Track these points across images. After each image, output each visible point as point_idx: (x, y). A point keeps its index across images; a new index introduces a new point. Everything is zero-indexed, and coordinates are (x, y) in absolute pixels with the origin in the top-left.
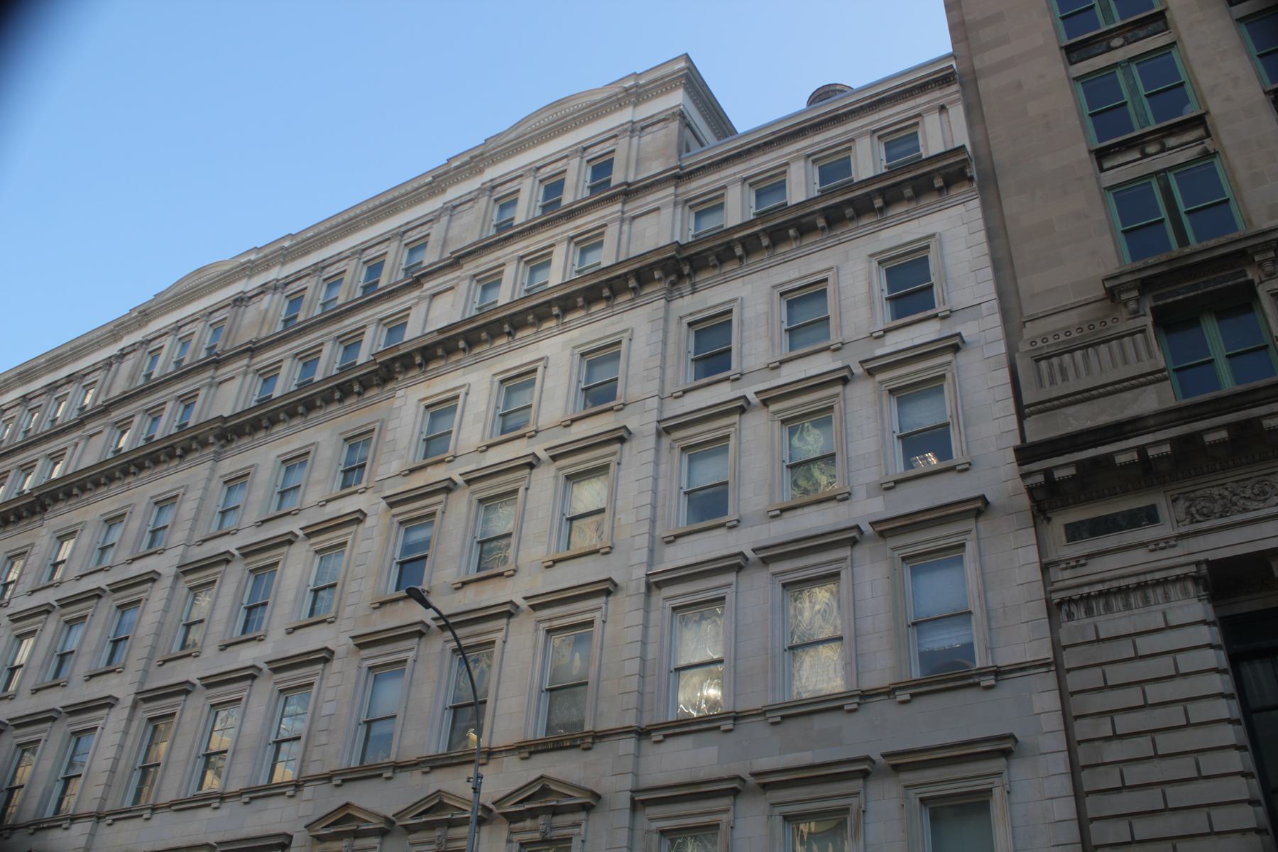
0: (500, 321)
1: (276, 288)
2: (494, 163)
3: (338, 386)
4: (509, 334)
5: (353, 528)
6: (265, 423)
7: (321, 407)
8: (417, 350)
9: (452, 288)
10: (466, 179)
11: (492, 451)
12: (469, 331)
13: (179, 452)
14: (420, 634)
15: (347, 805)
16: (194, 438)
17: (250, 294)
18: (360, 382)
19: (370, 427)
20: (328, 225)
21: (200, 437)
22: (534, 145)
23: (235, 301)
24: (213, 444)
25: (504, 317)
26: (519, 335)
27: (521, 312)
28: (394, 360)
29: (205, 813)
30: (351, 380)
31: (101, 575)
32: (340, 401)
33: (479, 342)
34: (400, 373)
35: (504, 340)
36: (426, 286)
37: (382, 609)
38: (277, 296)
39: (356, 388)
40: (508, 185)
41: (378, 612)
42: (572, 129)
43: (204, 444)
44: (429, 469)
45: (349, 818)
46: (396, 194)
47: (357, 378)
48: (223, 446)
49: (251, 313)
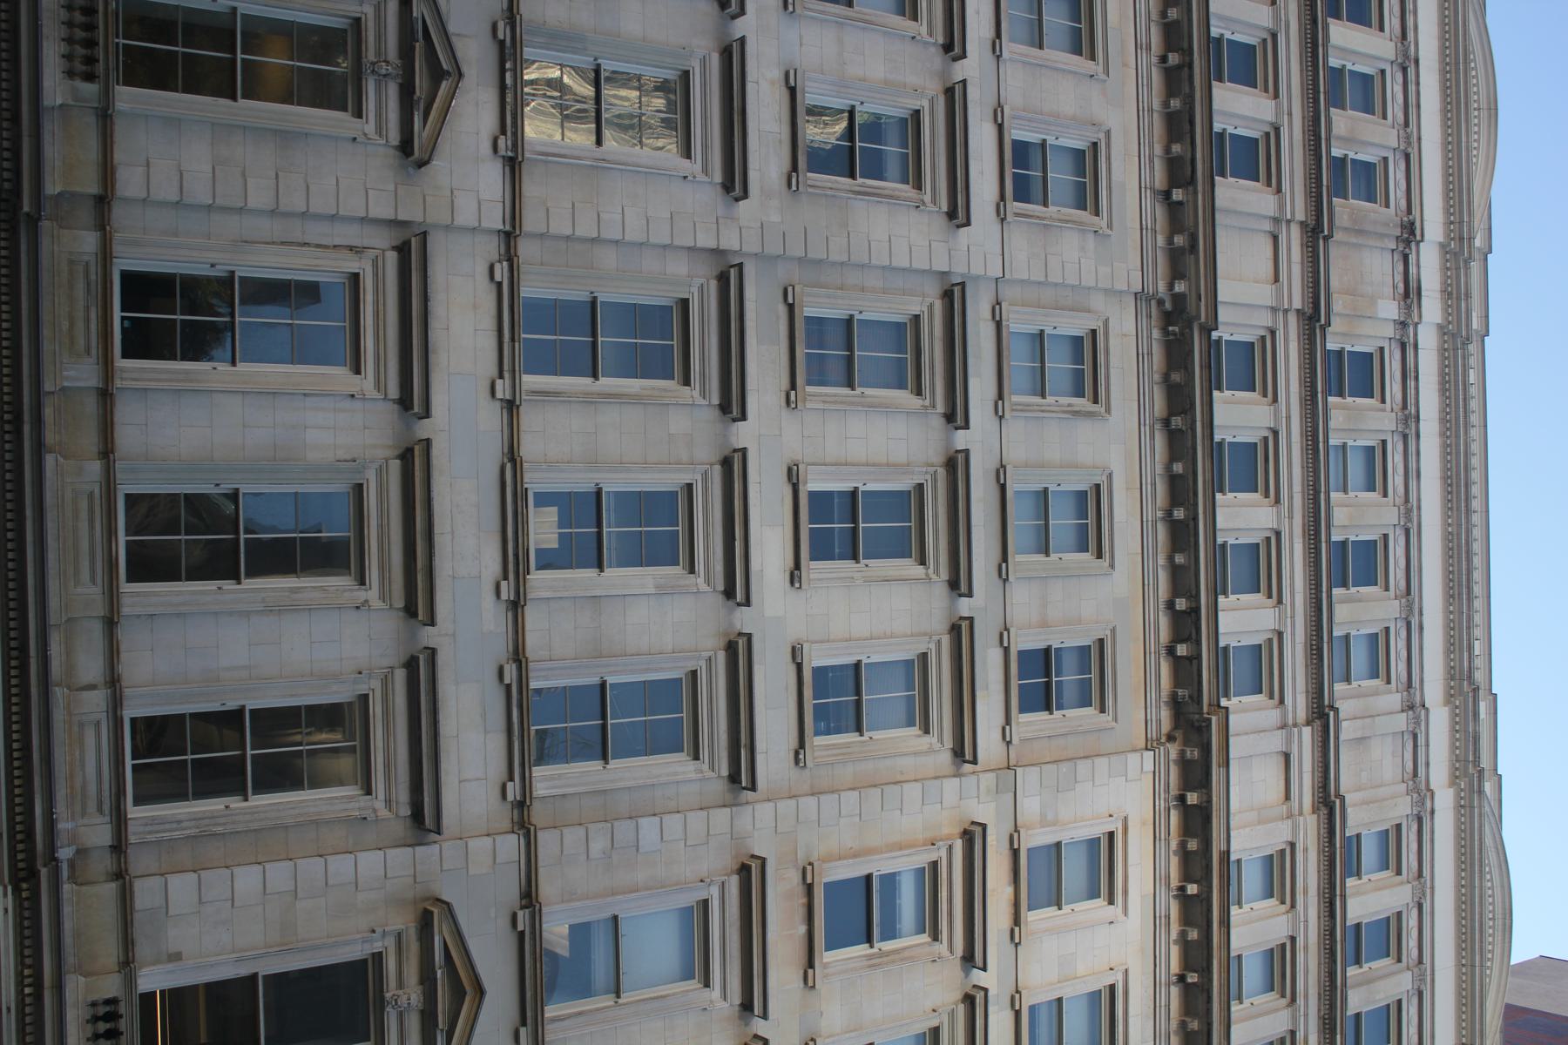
0: (1206, 971)
1: (1403, 325)
2: (1459, 807)
3: (1197, 610)
4: (1181, 978)
5: (949, 743)
6: (1177, 422)
7: (1170, 559)
8: (1209, 801)
9: (1287, 797)
10: (1453, 748)
11: (1009, 1016)
12: (1209, 910)
13: (1178, 195)
14: (747, 1006)
15: (480, 992)
16: (1193, 247)
17: (1412, 259)
18: (1189, 659)
19: (1109, 702)
20: (1475, 447)
21: (1190, 259)
22: (1459, 886)
23: (1412, 224)
24: (1171, 286)
25: (1210, 980)
26: (1175, 991)
27: (1209, 1012)
28: (1206, 749)
29: (491, 563)
30: (1198, 643)
31: (988, 32)
32: (1170, 605)
33: (1186, 920)
34: (1182, 753)
35: (1175, 967)
36: (1307, 731)
37: (800, 890)
38: (1389, 331)
39: (1182, 650)
40: (1414, 846)
41: (795, 877)
42: (1459, 956)
43: (1176, 273)
44: (1010, 890)
45: (458, 993)
46: (1477, 604)
47: (1199, 657)
48: (1160, 302)
49: (1379, 267)
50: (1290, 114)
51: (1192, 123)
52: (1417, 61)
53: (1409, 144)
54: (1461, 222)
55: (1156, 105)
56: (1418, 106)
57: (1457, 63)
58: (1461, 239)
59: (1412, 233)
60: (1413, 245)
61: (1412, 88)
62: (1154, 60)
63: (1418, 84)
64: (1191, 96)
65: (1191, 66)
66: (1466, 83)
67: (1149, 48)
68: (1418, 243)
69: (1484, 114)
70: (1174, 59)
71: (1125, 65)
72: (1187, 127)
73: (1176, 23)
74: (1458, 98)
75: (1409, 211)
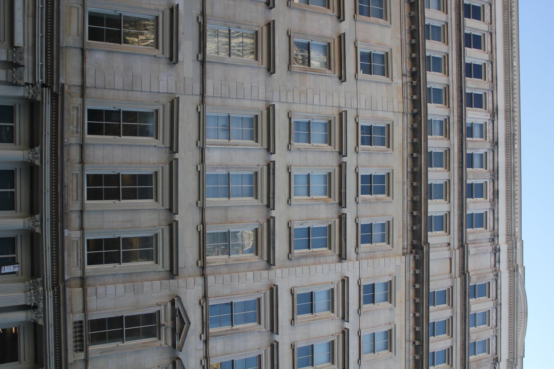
23: (497, 358)
31: (357, 358)
50: (456, 341)
51: (422, 364)
52: (501, 304)
53: (497, 332)
54: (514, 353)
55: (411, 357)
56: (501, 319)
57: (514, 302)
58: (514, 358)
59: (497, 361)
60: (497, 364)
61: (499, 313)
62: (411, 343)
63: (501, 311)
64: (423, 355)
65: (423, 346)
66: (517, 302)
67: (410, 341)
68: (499, 363)
69: (523, 314)
70: (417, 343)
71: (401, 348)
72: (421, 365)
73: (419, 332)
74: (514, 313)
75: (496, 354)
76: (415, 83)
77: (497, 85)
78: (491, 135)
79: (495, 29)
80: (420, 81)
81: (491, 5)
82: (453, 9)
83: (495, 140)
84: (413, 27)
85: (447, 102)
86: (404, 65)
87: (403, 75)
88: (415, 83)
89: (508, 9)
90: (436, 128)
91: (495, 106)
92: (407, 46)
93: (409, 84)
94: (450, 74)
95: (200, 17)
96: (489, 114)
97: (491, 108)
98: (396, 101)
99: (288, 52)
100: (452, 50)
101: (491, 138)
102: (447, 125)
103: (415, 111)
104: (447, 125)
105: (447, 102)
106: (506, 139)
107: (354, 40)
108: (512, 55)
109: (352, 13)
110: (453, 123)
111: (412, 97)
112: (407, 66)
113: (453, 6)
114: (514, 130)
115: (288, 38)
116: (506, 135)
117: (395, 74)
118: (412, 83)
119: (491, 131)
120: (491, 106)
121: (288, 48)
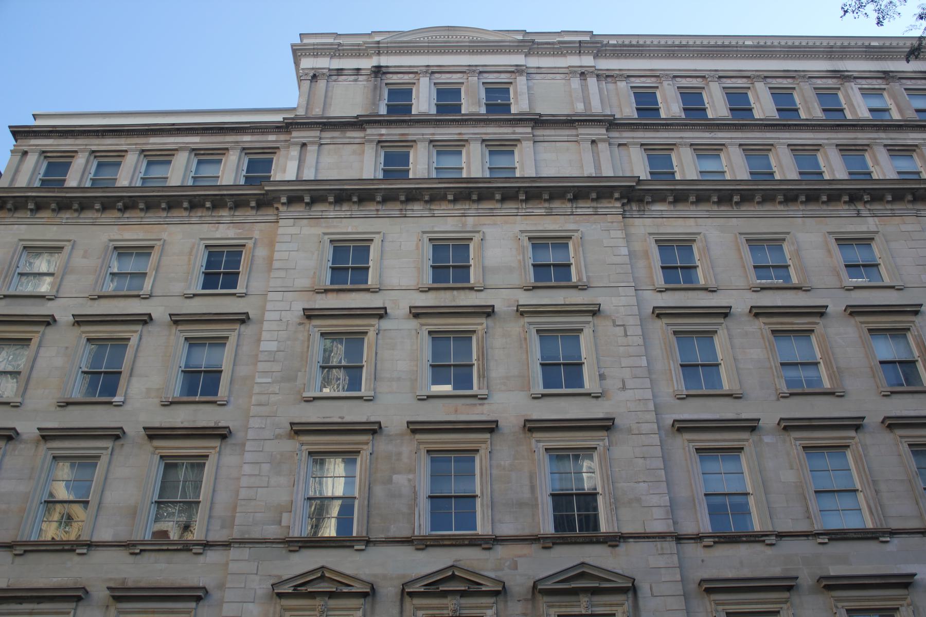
76: (866, 198)
77: (796, 71)
78: (874, 81)
79: (710, 71)
80: (864, 190)
81: (675, 77)
82: (712, 135)
83: (881, 75)
84: (780, 198)
85: (861, 148)
86: (843, 213)
87: (859, 215)
88: (866, 198)
89: (674, 51)
90: (710, 165)
91: (829, 74)
92: (809, 207)
93: (868, 206)
94: (771, 142)
95: (820, 541)
96: (847, 84)
97: (835, 80)
98: (904, 228)
99: (916, 396)
100: (779, 138)
101: (880, 81)
102: (897, 148)
103: (910, 197)
104: (897, 148)
105: (861, 148)
106: (872, 59)
107: (842, 292)
108: (805, 47)
109: (800, 293)
110: (891, 139)
111: (888, 202)
112: (842, 208)
113: (707, 135)
114: (863, 46)
115: (894, 396)
116: (866, 59)
117: (864, 229)
118: (866, 202)
119: (869, 81)
120: (830, 81)
121: (910, 396)
